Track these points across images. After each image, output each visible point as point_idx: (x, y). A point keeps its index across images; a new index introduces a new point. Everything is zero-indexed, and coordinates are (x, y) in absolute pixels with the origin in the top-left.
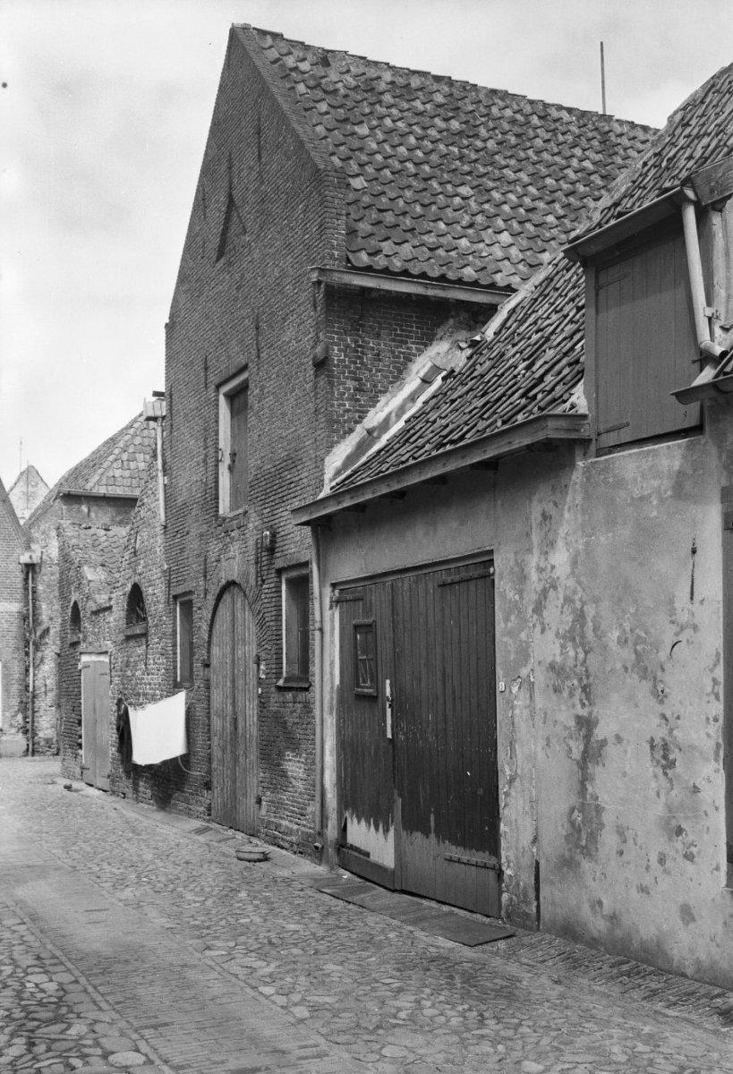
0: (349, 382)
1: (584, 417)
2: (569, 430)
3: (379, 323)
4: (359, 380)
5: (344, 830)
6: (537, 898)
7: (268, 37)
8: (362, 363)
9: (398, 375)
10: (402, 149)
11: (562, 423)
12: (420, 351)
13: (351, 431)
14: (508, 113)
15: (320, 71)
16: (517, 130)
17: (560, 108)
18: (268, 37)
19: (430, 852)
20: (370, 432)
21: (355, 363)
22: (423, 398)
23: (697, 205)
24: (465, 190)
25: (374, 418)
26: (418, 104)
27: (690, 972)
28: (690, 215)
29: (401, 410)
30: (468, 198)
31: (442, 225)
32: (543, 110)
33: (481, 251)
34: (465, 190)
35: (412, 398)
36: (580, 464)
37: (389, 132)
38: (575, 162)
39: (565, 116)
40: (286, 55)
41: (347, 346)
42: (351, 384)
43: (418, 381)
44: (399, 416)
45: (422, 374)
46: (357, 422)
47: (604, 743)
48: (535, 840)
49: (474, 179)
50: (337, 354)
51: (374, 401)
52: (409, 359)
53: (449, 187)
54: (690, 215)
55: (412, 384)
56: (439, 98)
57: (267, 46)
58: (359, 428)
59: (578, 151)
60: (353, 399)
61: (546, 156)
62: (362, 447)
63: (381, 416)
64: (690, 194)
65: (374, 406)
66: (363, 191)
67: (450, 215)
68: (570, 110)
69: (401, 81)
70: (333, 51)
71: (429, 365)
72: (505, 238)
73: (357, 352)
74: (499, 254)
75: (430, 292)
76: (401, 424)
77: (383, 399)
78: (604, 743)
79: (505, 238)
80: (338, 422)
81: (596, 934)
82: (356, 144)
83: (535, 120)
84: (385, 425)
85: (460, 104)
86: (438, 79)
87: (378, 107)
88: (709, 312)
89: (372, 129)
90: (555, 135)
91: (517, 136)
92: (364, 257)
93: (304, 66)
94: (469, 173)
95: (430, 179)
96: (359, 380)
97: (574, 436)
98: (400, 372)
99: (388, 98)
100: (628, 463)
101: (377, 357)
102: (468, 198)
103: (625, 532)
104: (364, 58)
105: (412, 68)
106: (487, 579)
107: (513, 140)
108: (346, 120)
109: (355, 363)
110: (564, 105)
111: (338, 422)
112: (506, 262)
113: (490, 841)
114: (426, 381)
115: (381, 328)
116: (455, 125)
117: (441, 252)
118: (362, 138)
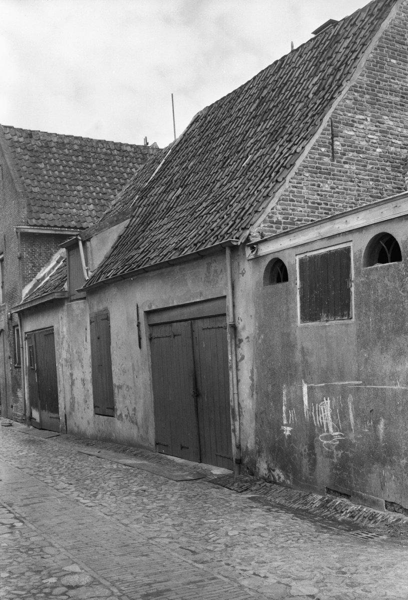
0: (30, 264)
1: (66, 292)
2: (61, 296)
3: (41, 243)
4: (33, 263)
5: (31, 413)
6: (66, 425)
7: (8, 129)
8: (34, 257)
9: (48, 260)
10: (56, 172)
11: (59, 294)
12: (56, 252)
13: (31, 280)
14: (104, 150)
15: (28, 141)
16: (107, 158)
17: (127, 145)
18: (8, 129)
19: (47, 414)
20: (38, 280)
21: (32, 257)
22: (56, 268)
23: (82, 240)
24: (79, 188)
25: (40, 275)
26: (66, 151)
27: (90, 437)
28: (80, 243)
29: (49, 272)
30: (80, 191)
31: (67, 204)
32: (119, 147)
33: (80, 213)
34: (79, 188)
35: (53, 268)
36: (66, 304)
37: (52, 165)
38: (128, 170)
39: (129, 149)
40: (14, 135)
41: (29, 252)
42: (31, 265)
43: (55, 262)
44: (48, 275)
45: (57, 260)
46: (33, 277)
47: (74, 380)
48: (65, 408)
49: (84, 182)
50: (25, 255)
51: (39, 270)
52: (52, 255)
53: (73, 187)
54: (80, 243)
55: (53, 263)
56: (76, 147)
57: (7, 132)
58: (34, 279)
59: (131, 165)
60: (31, 269)
61: (117, 168)
62: (35, 286)
63: (42, 275)
64: (80, 238)
65: (39, 272)
66: (38, 193)
67: (46, 223)
68: (131, 146)
69: (60, 141)
70: (34, 131)
71: (59, 256)
72: (92, 207)
73: (32, 254)
74: (87, 213)
75: (57, 233)
76: (48, 278)
77: (43, 269)
78: (74, 380)
79: (92, 207)
80: (26, 278)
81: (75, 432)
82: (38, 172)
83: (115, 152)
84: (43, 278)
85: (84, 148)
86: (77, 138)
87: (49, 154)
88: (86, 268)
89: (45, 164)
90: (123, 158)
91: (106, 160)
92: (34, 221)
93: (21, 140)
94: (82, 180)
95: (66, 184)
96: (33, 263)
97: (63, 297)
98: (49, 259)
99: (54, 150)
100: (75, 305)
101: (40, 255)
102: (80, 191)
103: (75, 323)
104: (46, 133)
105: (66, 134)
106: (107, 319)
107: (104, 162)
108: (35, 162)
109: (32, 257)
110: (129, 144)
111: (26, 278)
112: (90, 217)
113: (56, 410)
114: (58, 262)
115: (41, 245)
116: (80, 158)
117: (64, 216)
118: (41, 169)
